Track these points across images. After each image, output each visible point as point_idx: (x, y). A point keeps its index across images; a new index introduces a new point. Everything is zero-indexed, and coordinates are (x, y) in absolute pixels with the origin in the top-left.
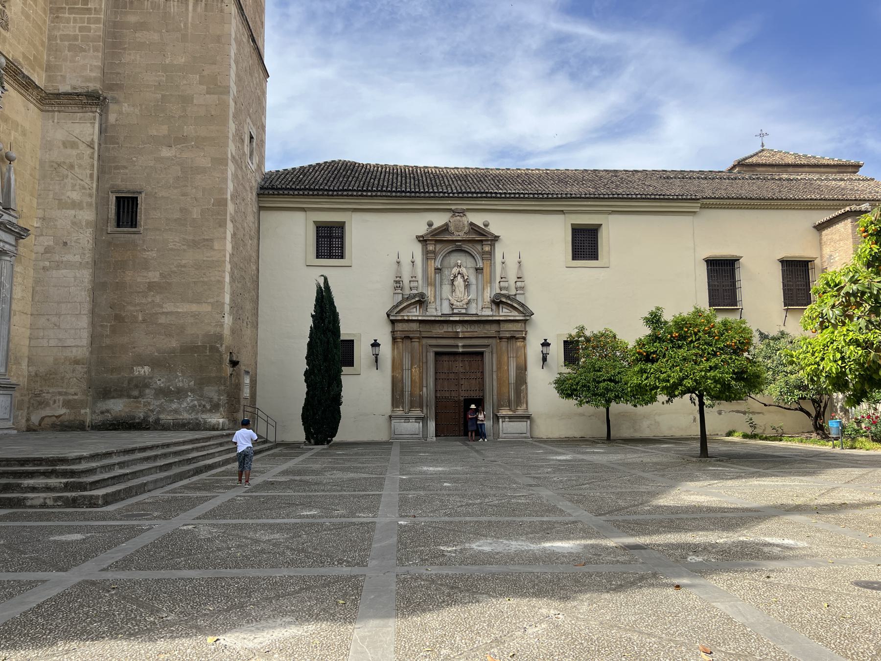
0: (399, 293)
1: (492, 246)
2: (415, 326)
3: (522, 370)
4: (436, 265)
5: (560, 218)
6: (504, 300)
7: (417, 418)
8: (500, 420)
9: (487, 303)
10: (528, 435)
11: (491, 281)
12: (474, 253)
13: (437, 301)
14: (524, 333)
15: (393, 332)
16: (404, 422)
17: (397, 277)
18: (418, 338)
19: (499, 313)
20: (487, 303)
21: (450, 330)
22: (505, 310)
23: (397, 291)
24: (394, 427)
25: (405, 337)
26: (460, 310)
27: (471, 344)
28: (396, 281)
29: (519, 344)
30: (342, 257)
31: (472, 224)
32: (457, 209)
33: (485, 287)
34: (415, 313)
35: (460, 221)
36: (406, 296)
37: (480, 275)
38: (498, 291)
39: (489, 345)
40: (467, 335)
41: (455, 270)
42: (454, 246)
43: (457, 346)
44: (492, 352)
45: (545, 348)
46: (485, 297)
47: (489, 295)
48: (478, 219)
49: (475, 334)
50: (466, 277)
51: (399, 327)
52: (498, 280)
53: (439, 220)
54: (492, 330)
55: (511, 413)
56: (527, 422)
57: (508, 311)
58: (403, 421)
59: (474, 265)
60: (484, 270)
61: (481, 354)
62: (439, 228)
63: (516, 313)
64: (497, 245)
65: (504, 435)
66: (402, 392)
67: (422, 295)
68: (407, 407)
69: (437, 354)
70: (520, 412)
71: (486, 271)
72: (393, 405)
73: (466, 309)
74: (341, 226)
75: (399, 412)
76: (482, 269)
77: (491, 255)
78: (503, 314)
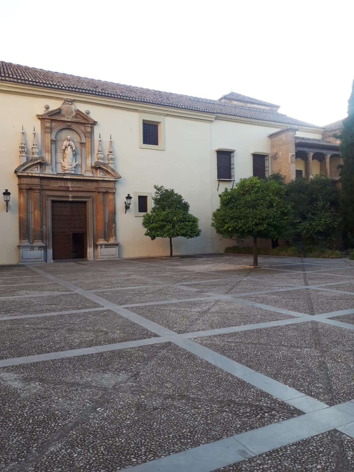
0: (24, 156)
1: (92, 128)
2: (37, 181)
3: (114, 213)
4: (52, 137)
5: (136, 114)
6: (102, 166)
7: (40, 248)
8: (99, 247)
9: (89, 168)
10: (117, 256)
11: (92, 152)
12: (80, 132)
13: (53, 163)
14: (114, 189)
15: (19, 184)
16: (30, 250)
17: (22, 144)
18: (39, 190)
19: (97, 175)
20: (89, 168)
21: (63, 185)
22: (101, 174)
23: (22, 155)
24: (23, 254)
25: (29, 188)
26: (70, 171)
27: (78, 196)
28: (22, 147)
29: (111, 197)
31: (78, 111)
32: (67, 99)
33: (88, 156)
34: (36, 172)
35: (69, 108)
36: (30, 159)
37: (84, 148)
38: (96, 160)
39: (91, 197)
40: (75, 189)
41: (66, 143)
42: (66, 125)
43: (68, 197)
44: (93, 202)
45: (129, 200)
46: (88, 164)
47: (90, 162)
48: (83, 108)
49: (81, 189)
50: (74, 149)
51: (25, 181)
52: (96, 152)
53: (55, 105)
54: (92, 186)
55: (106, 242)
56: (116, 247)
57: (103, 174)
58: (29, 249)
59: (79, 140)
60: (87, 144)
61: (85, 202)
62: (55, 111)
63: (109, 176)
64: (96, 129)
65: (102, 257)
67: (42, 158)
68: (31, 240)
69: (53, 202)
70: (112, 241)
71: (88, 145)
72: (20, 238)
73: (74, 171)
75: (26, 243)
76: (85, 144)
77: (91, 135)
78: (101, 176)
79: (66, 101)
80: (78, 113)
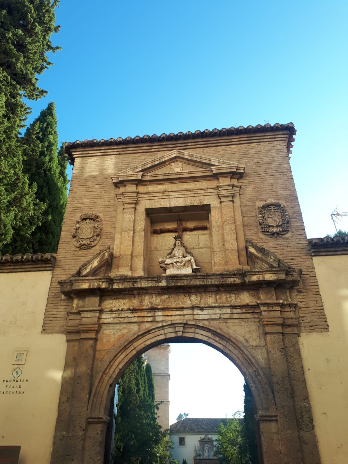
15: (195, 462)
30: (184, 445)
34: (198, 458)
41: (206, 448)
48: (210, 436)
51: (196, 461)
53: (203, 437)
74: (184, 438)
79: (205, 435)
80: (209, 438)
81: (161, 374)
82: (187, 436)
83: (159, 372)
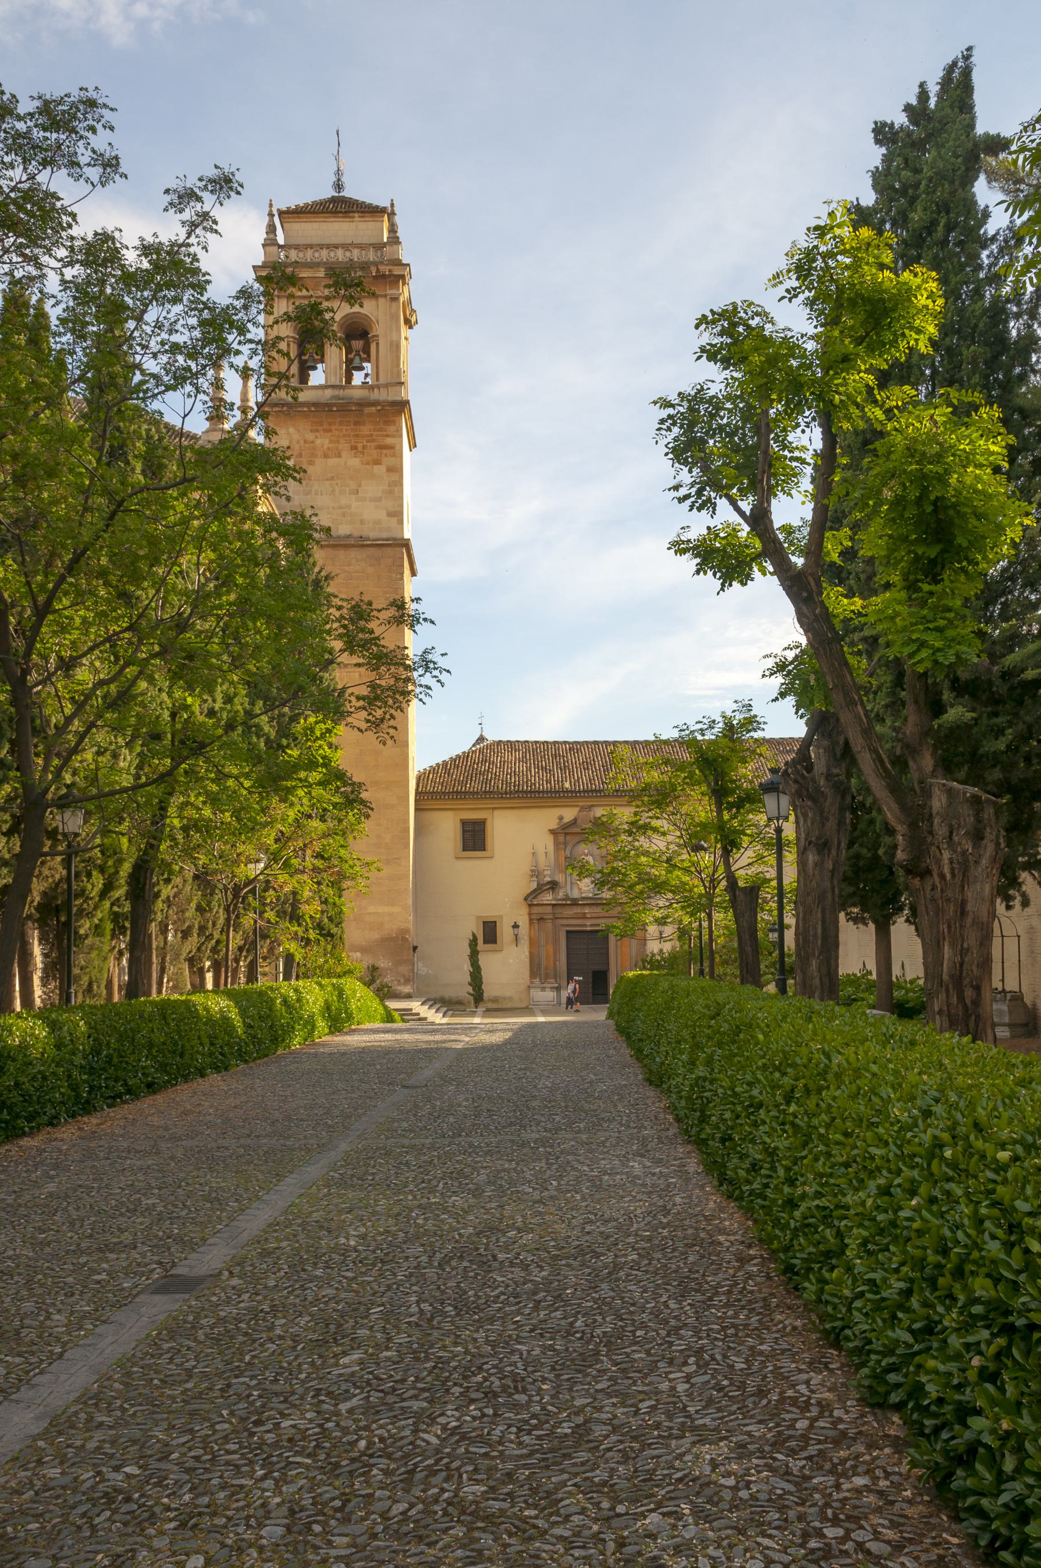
15: (530, 914)
51: (535, 910)
53: (569, 814)
66: (539, 965)
69: (568, 932)
81: (368, 539)
82: (497, 813)
83: (356, 534)
